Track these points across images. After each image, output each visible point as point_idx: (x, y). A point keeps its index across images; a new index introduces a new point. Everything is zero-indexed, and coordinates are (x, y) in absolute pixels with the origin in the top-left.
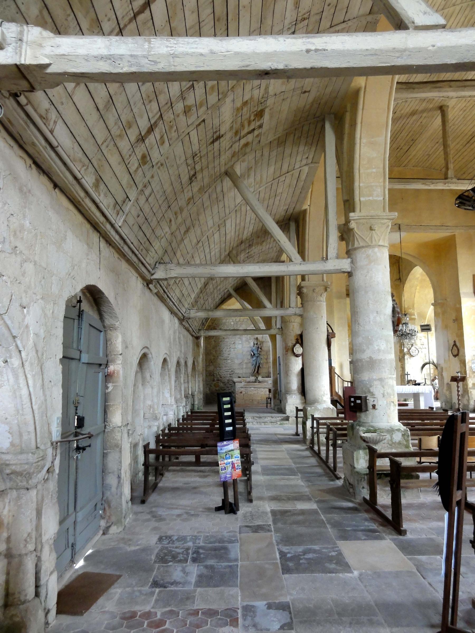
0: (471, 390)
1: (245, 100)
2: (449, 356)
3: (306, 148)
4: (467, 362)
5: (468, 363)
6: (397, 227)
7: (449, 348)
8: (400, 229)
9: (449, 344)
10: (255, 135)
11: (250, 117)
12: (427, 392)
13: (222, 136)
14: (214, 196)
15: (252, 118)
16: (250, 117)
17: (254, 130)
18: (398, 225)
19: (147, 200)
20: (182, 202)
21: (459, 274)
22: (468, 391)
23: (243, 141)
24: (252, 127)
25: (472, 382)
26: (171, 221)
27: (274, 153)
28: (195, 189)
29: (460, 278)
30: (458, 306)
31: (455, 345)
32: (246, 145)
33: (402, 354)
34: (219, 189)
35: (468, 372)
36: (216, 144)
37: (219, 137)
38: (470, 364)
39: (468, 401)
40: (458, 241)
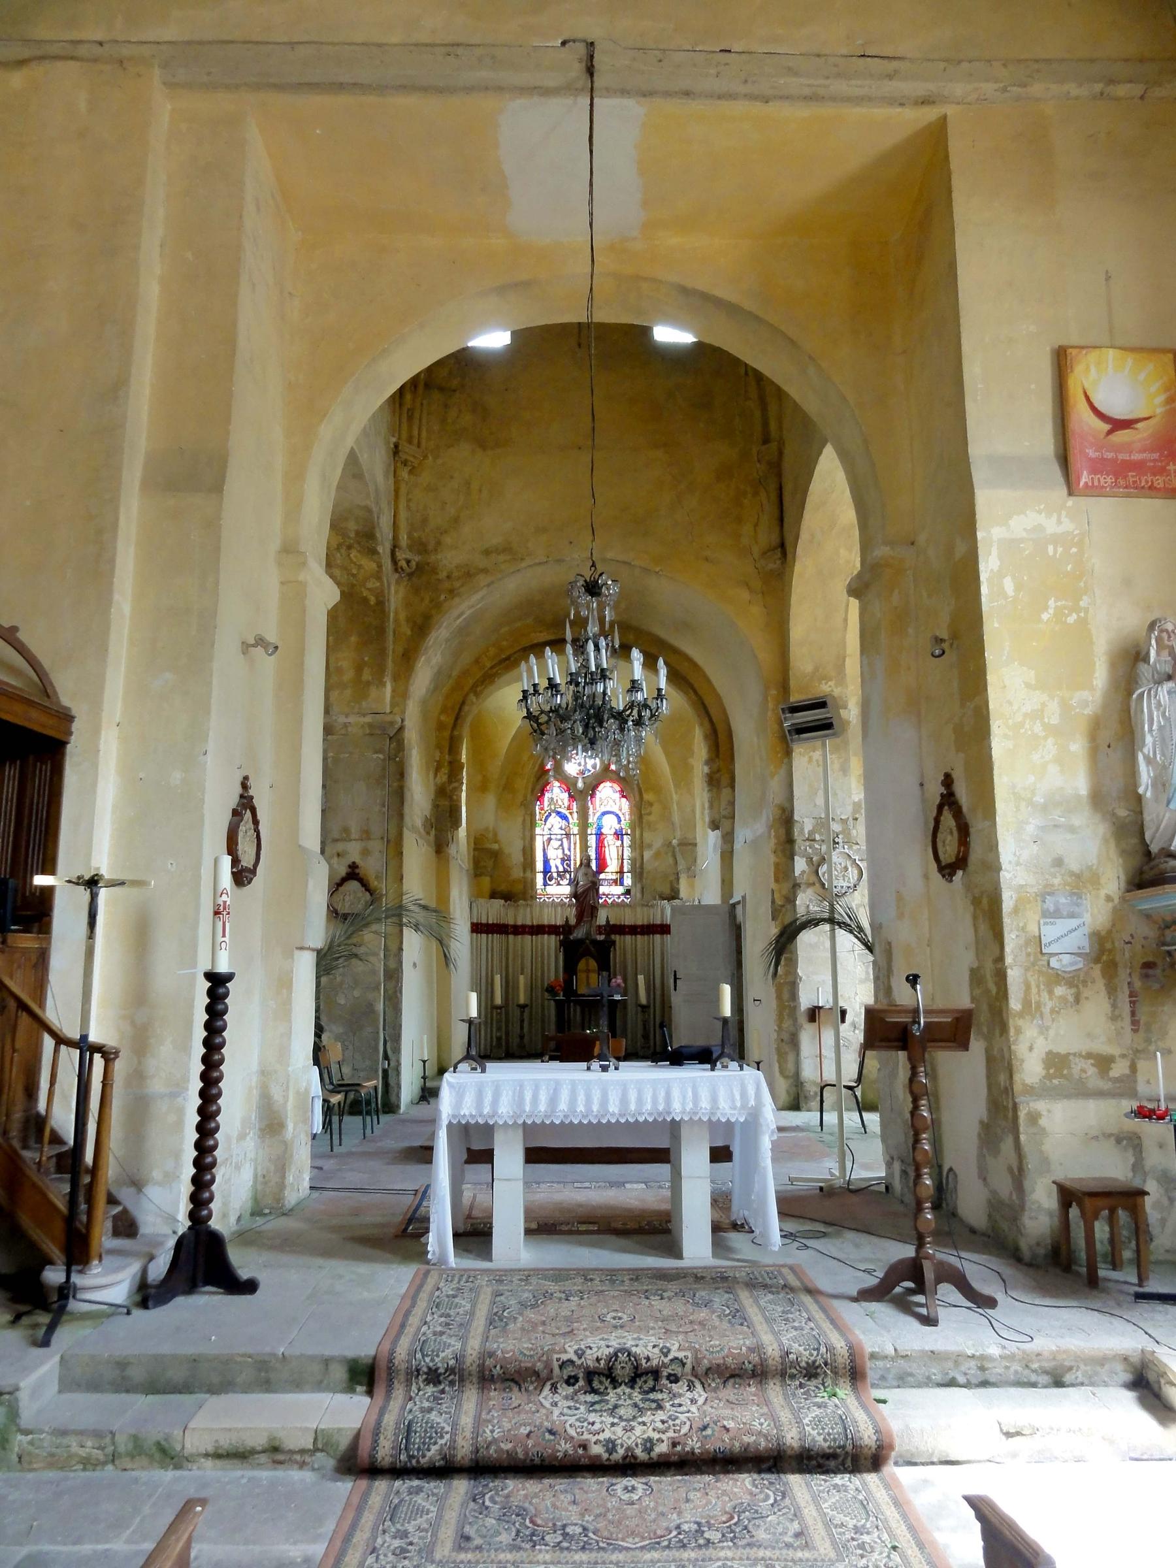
0: (1040, 1106)
2: (926, 877)
4: (1008, 900)
5: (1016, 910)
6: (573, 58)
7: (926, 823)
8: (590, 71)
9: (924, 800)
12: (728, 1110)
18: (581, 49)
21: (966, 347)
22: (1015, 1108)
25: (1042, 1046)
29: (973, 371)
30: (961, 549)
31: (949, 800)
33: (786, 887)
35: (1014, 975)
38: (1032, 921)
39: (1018, 1175)
40: (956, 147)
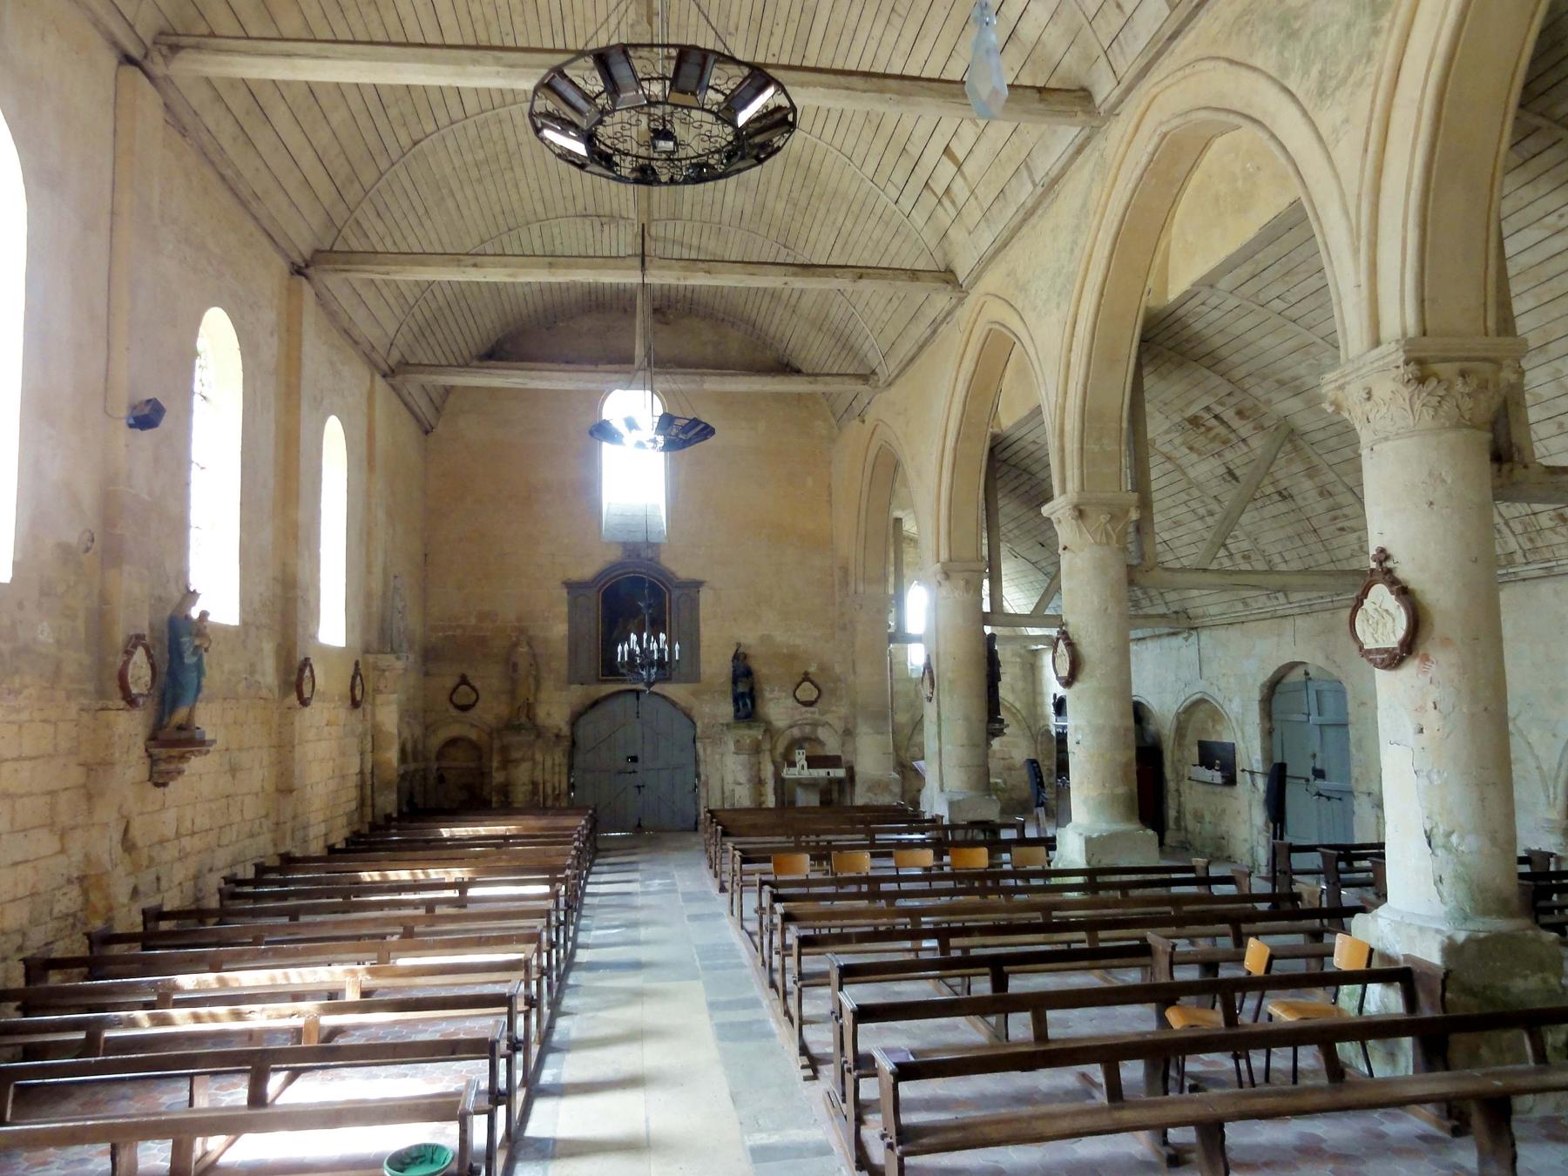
1: (1187, 451)
3: (1191, 321)
10: (1222, 409)
11: (1202, 433)
13: (1228, 468)
14: (1333, 442)
15: (1203, 429)
16: (1202, 433)
17: (1216, 417)
19: (1286, 562)
20: (1320, 506)
23: (1236, 423)
24: (1214, 422)
26: (1342, 529)
27: (1236, 358)
28: (1307, 484)
32: (1240, 414)
34: (1320, 436)
36: (1238, 472)
37: (1230, 473)
